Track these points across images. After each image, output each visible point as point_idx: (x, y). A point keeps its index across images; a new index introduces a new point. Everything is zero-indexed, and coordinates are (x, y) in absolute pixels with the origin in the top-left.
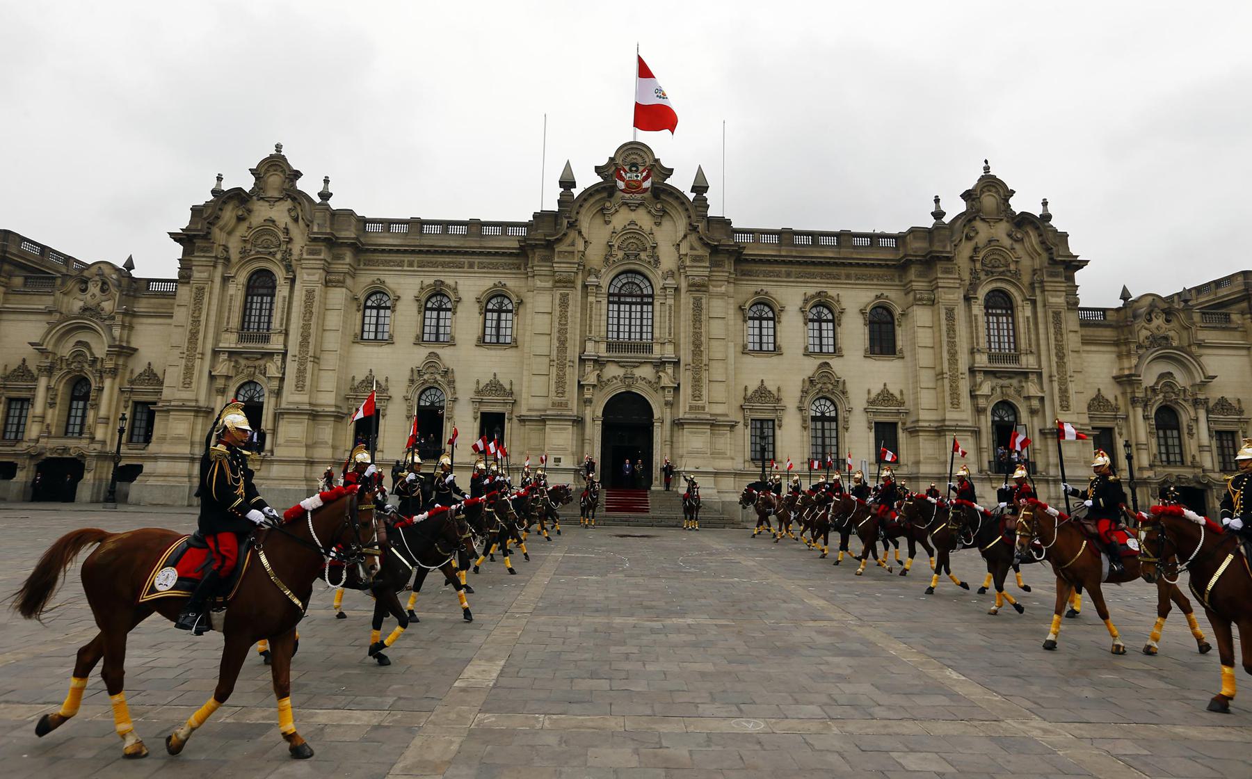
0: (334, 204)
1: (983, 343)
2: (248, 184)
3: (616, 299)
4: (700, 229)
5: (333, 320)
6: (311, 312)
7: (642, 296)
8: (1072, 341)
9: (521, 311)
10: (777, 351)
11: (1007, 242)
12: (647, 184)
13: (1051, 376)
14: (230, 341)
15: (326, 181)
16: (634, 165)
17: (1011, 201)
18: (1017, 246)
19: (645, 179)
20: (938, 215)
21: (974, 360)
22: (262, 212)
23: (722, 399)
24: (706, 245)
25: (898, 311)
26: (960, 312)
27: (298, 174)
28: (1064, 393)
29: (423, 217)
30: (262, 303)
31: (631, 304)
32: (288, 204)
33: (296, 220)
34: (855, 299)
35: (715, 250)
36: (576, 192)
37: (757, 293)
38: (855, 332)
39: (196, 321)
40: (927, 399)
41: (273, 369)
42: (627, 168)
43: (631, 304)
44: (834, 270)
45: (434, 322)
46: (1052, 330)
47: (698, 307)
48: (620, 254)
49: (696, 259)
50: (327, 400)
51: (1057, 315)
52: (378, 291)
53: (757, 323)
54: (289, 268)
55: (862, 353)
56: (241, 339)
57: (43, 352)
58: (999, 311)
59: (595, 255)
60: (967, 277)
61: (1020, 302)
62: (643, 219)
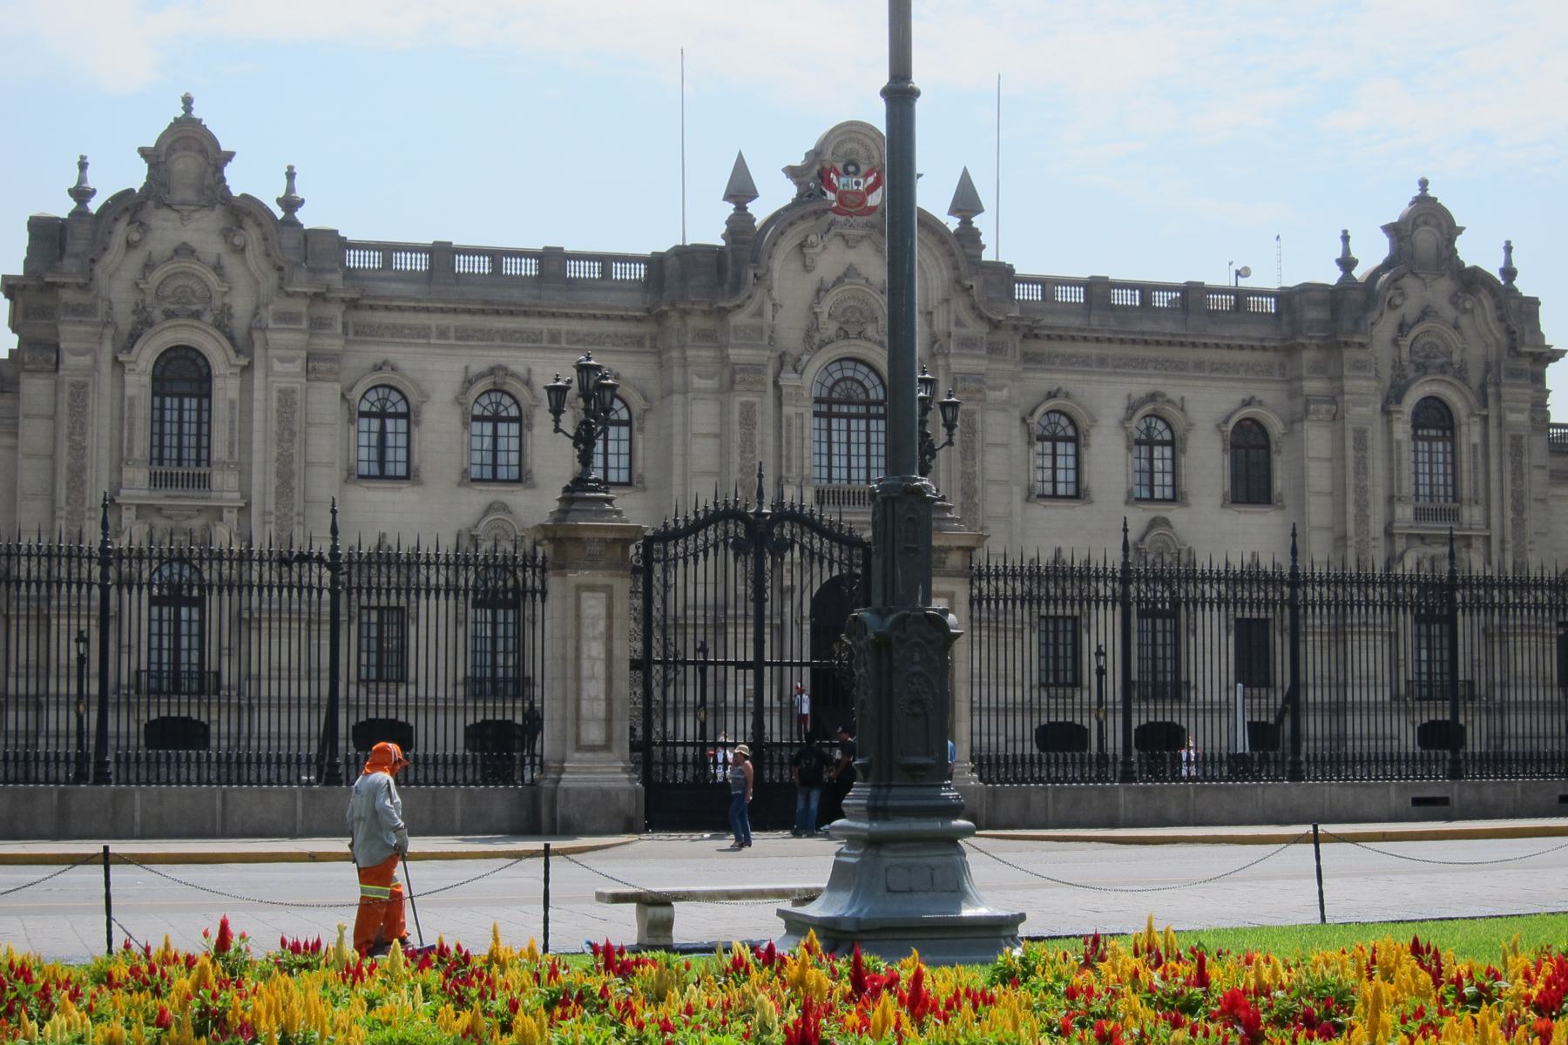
0: (308, 218)
1: (1407, 488)
3: (824, 408)
4: (975, 292)
6: (292, 434)
7: (868, 403)
8: (1537, 481)
9: (650, 424)
10: (1079, 494)
11: (1449, 313)
12: (874, 199)
13: (1503, 542)
15: (291, 175)
16: (852, 163)
19: (871, 189)
20: (1347, 263)
21: (1392, 513)
24: (981, 317)
25: (1276, 427)
27: (230, 156)
29: (458, 241)
30: (181, 410)
31: (849, 417)
33: (241, 250)
35: (995, 326)
37: (1051, 395)
38: (1207, 463)
39: (78, 450)
42: (840, 167)
43: (849, 417)
45: (487, 443)
46: (1508, 467)
48: (831, 328)
49: (967, 343)
51: (1517, 441)
53: (1048, 445)
55: (1219, 501)
56: (156, 480)
58: (1433, 432)
60: (1387, 373)
61: (1464, 419)
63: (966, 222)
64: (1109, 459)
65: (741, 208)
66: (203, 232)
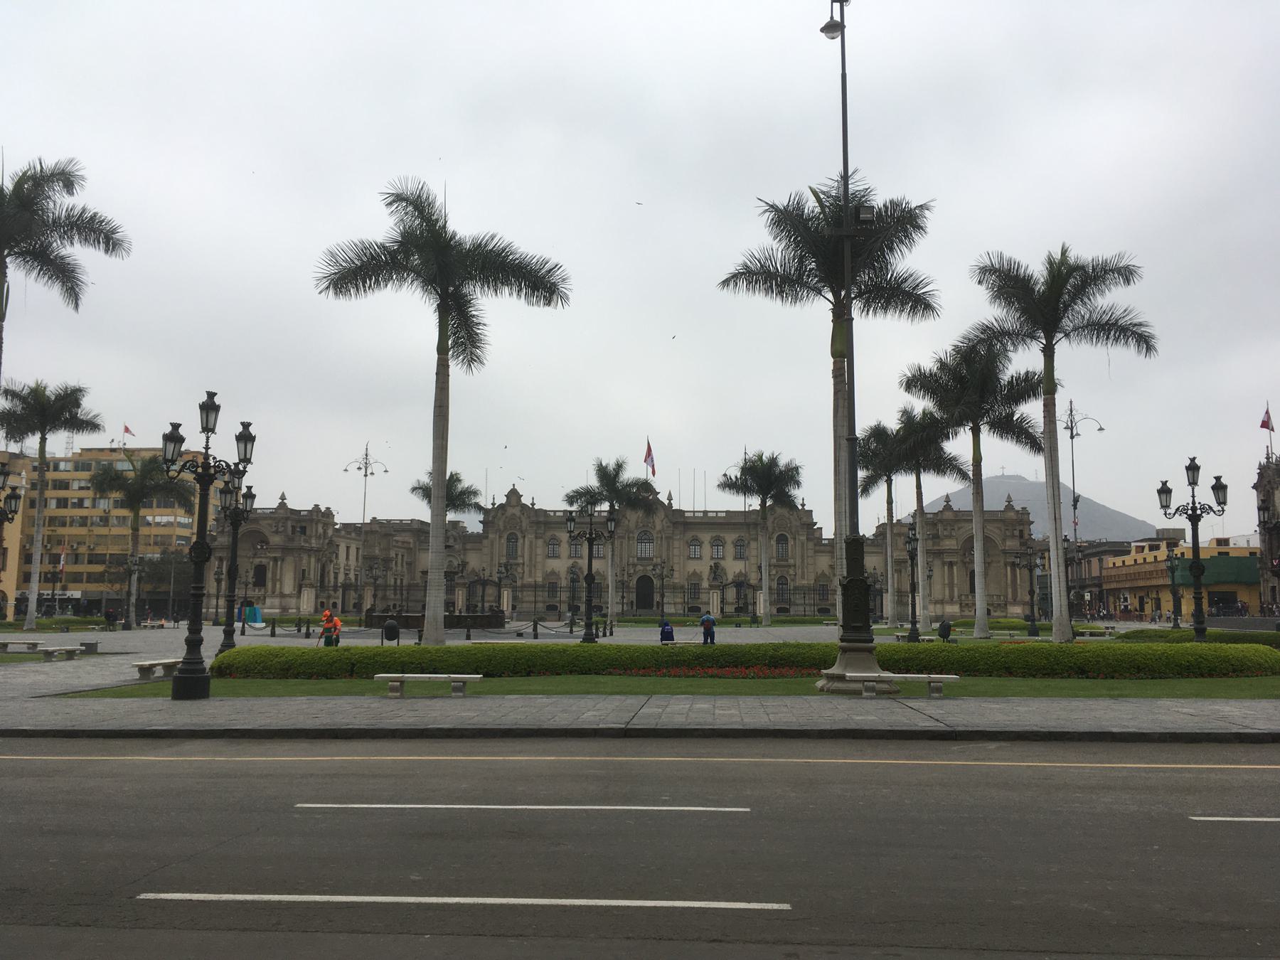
2: (504, 500)
5: (539, 551)
10: (701, 558)
22: (510, 511)
23: (678, 578)
28: (803, 573)
34: (730, 537)
35: (674, 524)
38: (730, 550)
41: (520, 570)
50: (540, 579)
52: (554, 538)
59: (632, 525)
64: (707, 550)
66: (517, 511)
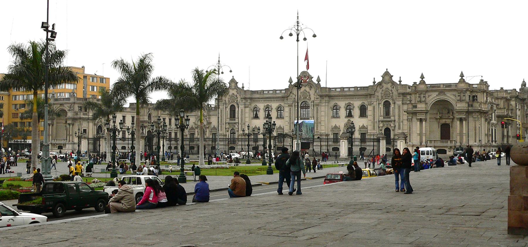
5: (247, 115)
10: (339, 117)
11: (390, 88)
14: (228, 121)
17: (393, 78)
18: (393, 89)
26: (377, 107)
28: (399, 125)
32: (236, 90)
35: (321, 96)
36: (292, 84)
38: (356, 112)
40: (370, 128)
41: (236, 127)
44: (352, 97)
47: (317, 108)
49: (317, 98)
51: (399, 106)
54: (238, 104)
56: (230, 120)
57: (195, 124)
62: (307, 89)
63: (318, 82)
65: (291, 83)
